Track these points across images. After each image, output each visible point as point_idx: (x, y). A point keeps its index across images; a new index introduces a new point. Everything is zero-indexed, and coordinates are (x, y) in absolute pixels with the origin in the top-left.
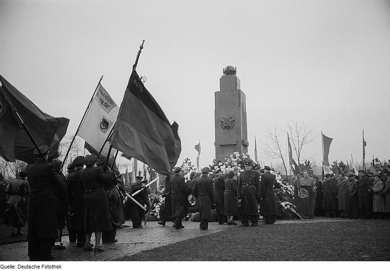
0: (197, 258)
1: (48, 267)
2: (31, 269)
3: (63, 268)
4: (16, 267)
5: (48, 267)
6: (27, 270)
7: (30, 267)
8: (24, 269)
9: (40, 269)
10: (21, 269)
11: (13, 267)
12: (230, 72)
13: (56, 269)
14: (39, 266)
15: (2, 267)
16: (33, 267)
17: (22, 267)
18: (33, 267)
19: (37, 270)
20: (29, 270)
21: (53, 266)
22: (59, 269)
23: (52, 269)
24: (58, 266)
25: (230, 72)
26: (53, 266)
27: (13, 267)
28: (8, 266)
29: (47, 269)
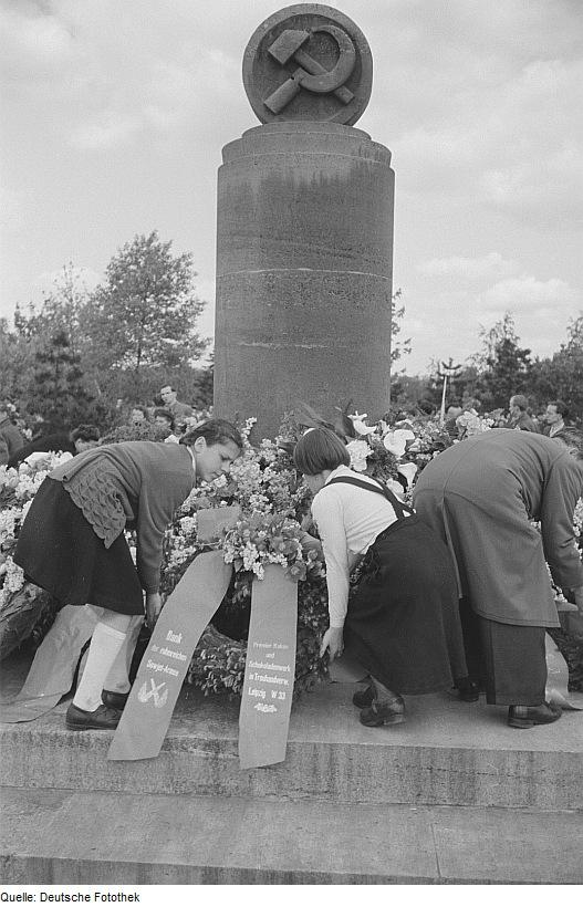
0: (221, 226)
3: (143, 900)
4: (37, 898)
5: (108, 898)
7: (68, 898)
11: (29, 898)
12: (309, 72)
14: (88, 897)
15: (5, 897)
16: (75, 898)
17: (51, 898)
18: (75, 898)
21: (120, 897)
24: (131, 897)
26: (120, 897)
27: (29, 898)
28: (19, 897)
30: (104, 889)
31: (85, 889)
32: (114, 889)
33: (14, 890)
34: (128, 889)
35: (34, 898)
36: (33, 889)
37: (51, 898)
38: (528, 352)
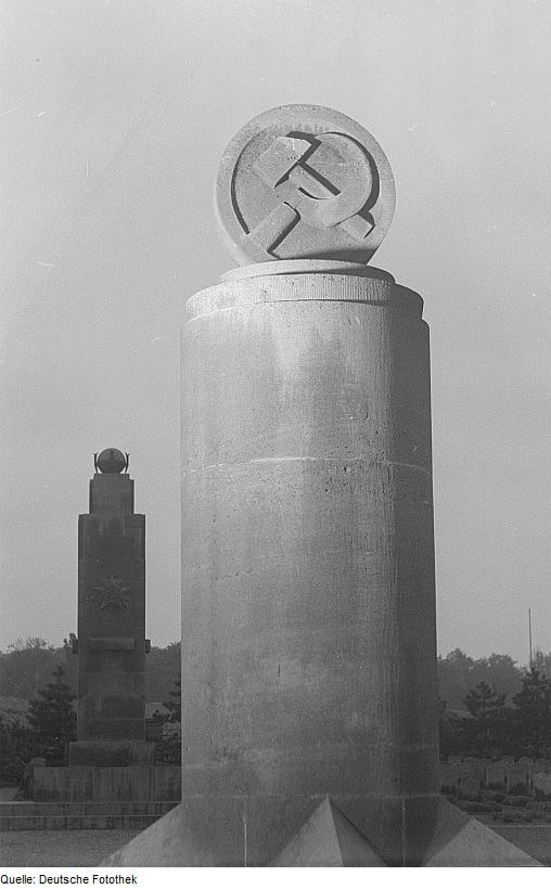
1: (105, 880)
3: (140, 883)
4: (37, 880)
5: (105, 880)
6: (59, 886)
8: (53, 886)
9: (90, 885)
10: (47, 885)
11: (28, 880)
12: (112, 464)
13: (125, 886)
14: (86, 879)
15: (4, 879)
16: (73, 880)
17: (50, 880)
18: (73, 880)
19: (83, 886)
20: (64, 886)
21: (118, 879)
22: (131, 886)
23: (115, 886)
24: (128, 879)
25: (112, 464)
26: (118, 879)
27: (28, 880)
28: (19, 879)
29: (105, 886)
30: (102, 871)
31: (83, 872)
32: (112, 871)
33: (14, 872)
34: (125, 872)
35: (34, 880)
37: (50, 880)
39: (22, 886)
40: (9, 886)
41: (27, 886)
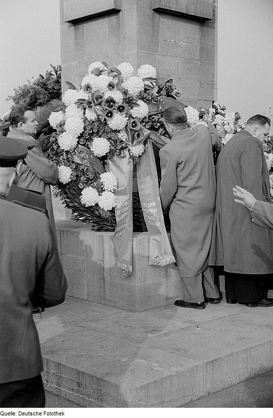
1: (50, 414)
2: (33, 416)
3: (66, 415)
4: (17, 414)
5: (50, 414)
6: (28, 416)
8: (25, 416)
9: (42, 416)
10: (22, 416)
11: (13, 414)
13: (59, 416)
14: (40, 413)
15: (2, 413)
16: (35, 414)
17: (23, 414)
18: (35, 414)
19: (39, 416)
20: (30, 417)
21: (56, 413)
22: (62, 416)
23: (54, 416)
24: (60, 413)
26: (56, 413)
27: (13, 414)
28: (9, 413)
29: (49, 416)
32: (53, 410)
34: (59, 410)
35: (16, 414)
36: (15, 410)
38: (82, 195)
39: (10, 416)
40: (4, 416)
41: (13, 416)
